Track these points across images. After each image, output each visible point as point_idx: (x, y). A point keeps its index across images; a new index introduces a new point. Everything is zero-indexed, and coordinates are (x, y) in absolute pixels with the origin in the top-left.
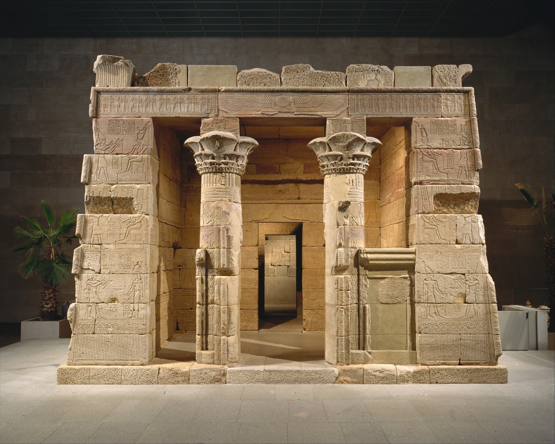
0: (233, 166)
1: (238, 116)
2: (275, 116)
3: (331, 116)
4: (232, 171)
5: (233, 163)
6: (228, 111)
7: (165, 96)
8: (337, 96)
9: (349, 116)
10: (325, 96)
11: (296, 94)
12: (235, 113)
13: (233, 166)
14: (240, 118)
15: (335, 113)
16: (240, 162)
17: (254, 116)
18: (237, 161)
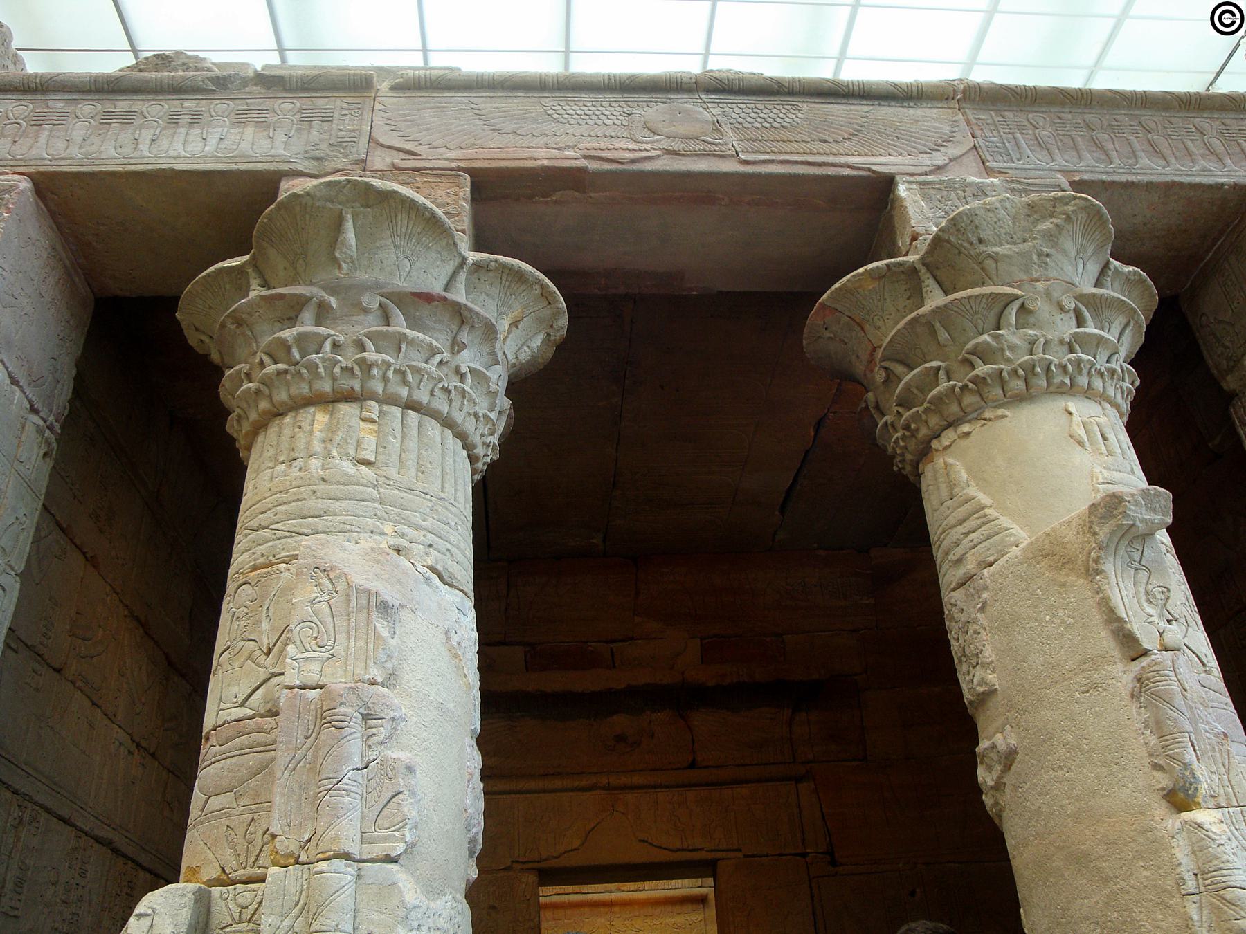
0: (432, 367)
1: (462, 164)
2: (647, 166)
3: (911, 169)
4: (423, 396)
5: (434, 352)
6: (418, 149)
7: (123, 105)
8: (914, 112)
9: (990, 172)
10: (866, 108)
11: (738, 99)
12: (452, 155)
13: (432, 367)
14: (471, 172)
15: (927, 161)
16: (468, 359)
17: (546, 163)
18: (456, 347)
